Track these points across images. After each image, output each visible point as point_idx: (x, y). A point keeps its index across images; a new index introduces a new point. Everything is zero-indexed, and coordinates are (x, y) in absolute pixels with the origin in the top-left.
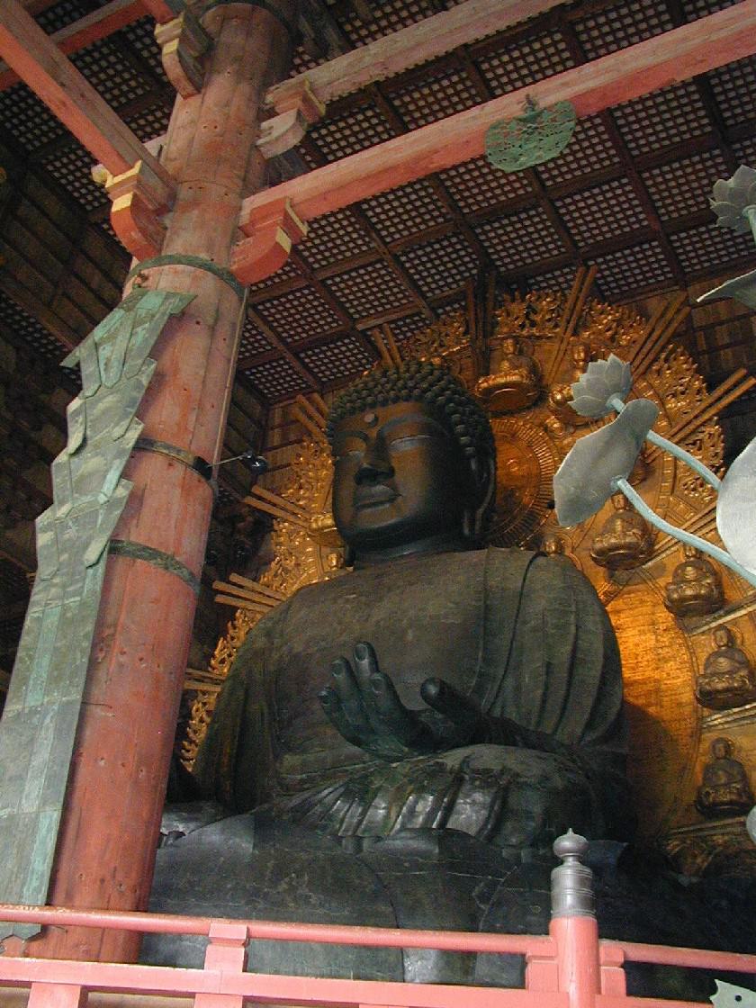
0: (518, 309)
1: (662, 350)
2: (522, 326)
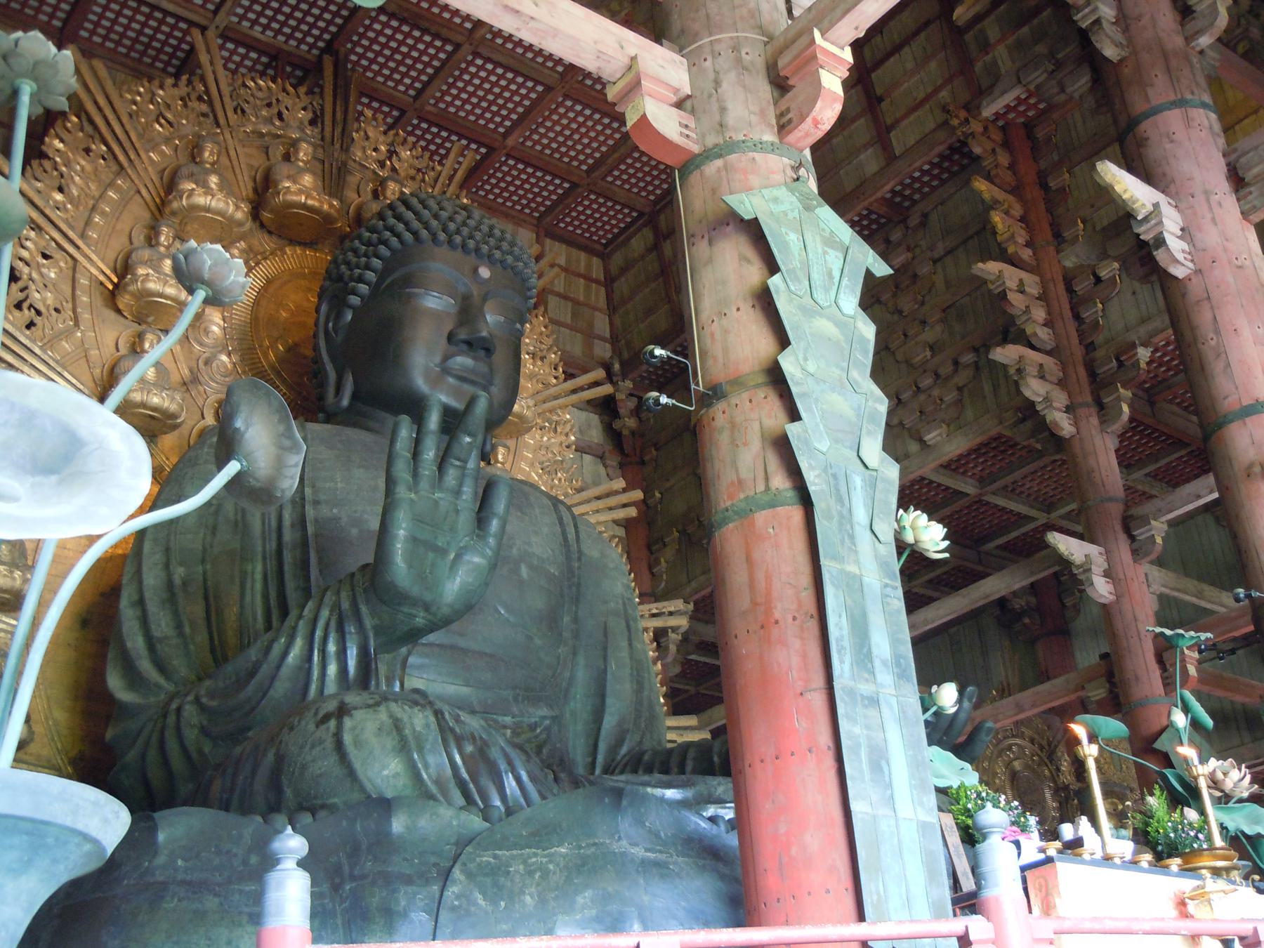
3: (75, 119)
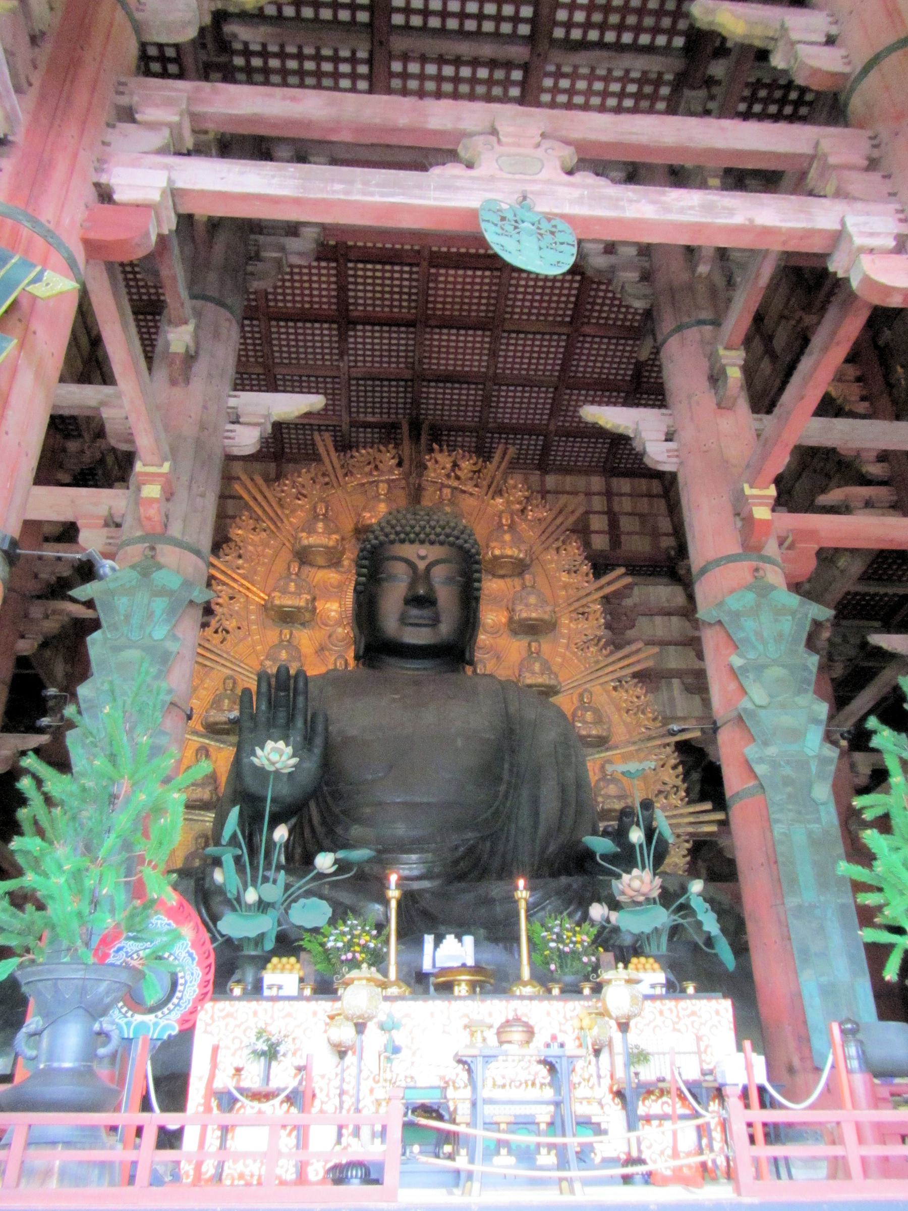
0: (445, 459)
2: (448, 476)
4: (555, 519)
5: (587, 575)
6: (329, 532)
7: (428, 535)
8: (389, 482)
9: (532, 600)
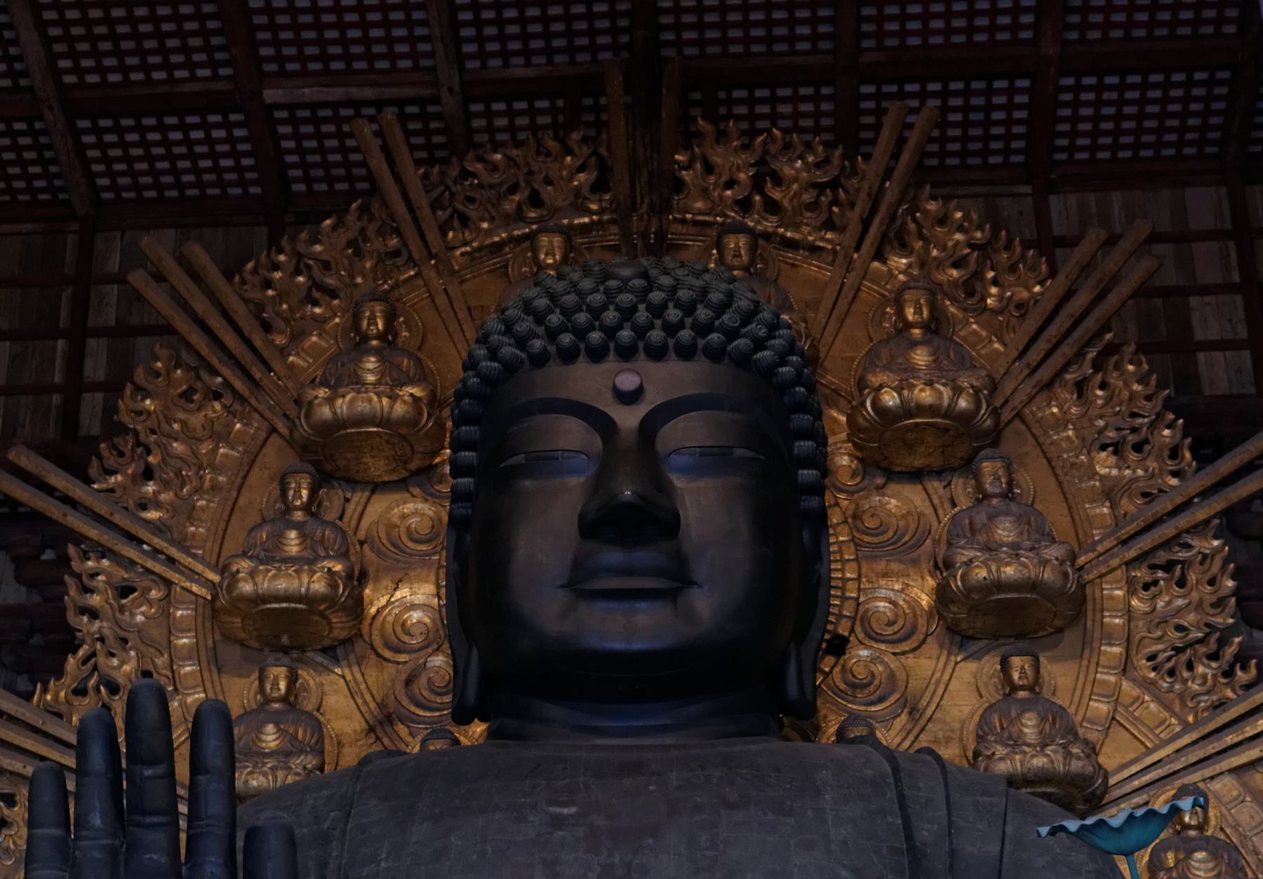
0: (734, 161)
1: (1089, 343)
2: (744, 205)
3: (164, 353)
4: (1069, 295)
5: (1174, 453)
6: (393, 380)
7: (641, 332)
8: (568, 233)
9: (1005, 531)
